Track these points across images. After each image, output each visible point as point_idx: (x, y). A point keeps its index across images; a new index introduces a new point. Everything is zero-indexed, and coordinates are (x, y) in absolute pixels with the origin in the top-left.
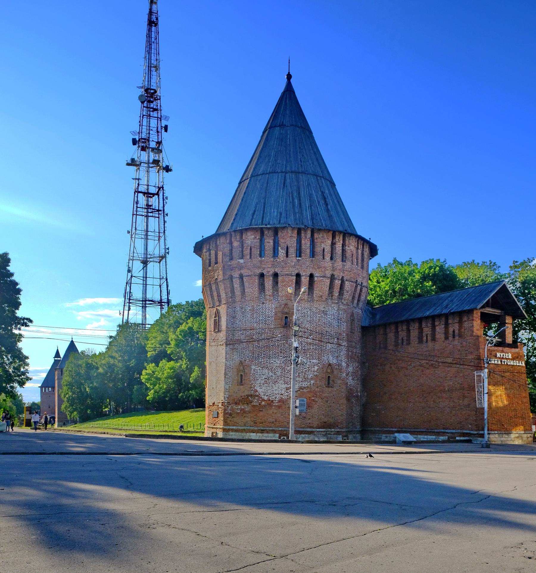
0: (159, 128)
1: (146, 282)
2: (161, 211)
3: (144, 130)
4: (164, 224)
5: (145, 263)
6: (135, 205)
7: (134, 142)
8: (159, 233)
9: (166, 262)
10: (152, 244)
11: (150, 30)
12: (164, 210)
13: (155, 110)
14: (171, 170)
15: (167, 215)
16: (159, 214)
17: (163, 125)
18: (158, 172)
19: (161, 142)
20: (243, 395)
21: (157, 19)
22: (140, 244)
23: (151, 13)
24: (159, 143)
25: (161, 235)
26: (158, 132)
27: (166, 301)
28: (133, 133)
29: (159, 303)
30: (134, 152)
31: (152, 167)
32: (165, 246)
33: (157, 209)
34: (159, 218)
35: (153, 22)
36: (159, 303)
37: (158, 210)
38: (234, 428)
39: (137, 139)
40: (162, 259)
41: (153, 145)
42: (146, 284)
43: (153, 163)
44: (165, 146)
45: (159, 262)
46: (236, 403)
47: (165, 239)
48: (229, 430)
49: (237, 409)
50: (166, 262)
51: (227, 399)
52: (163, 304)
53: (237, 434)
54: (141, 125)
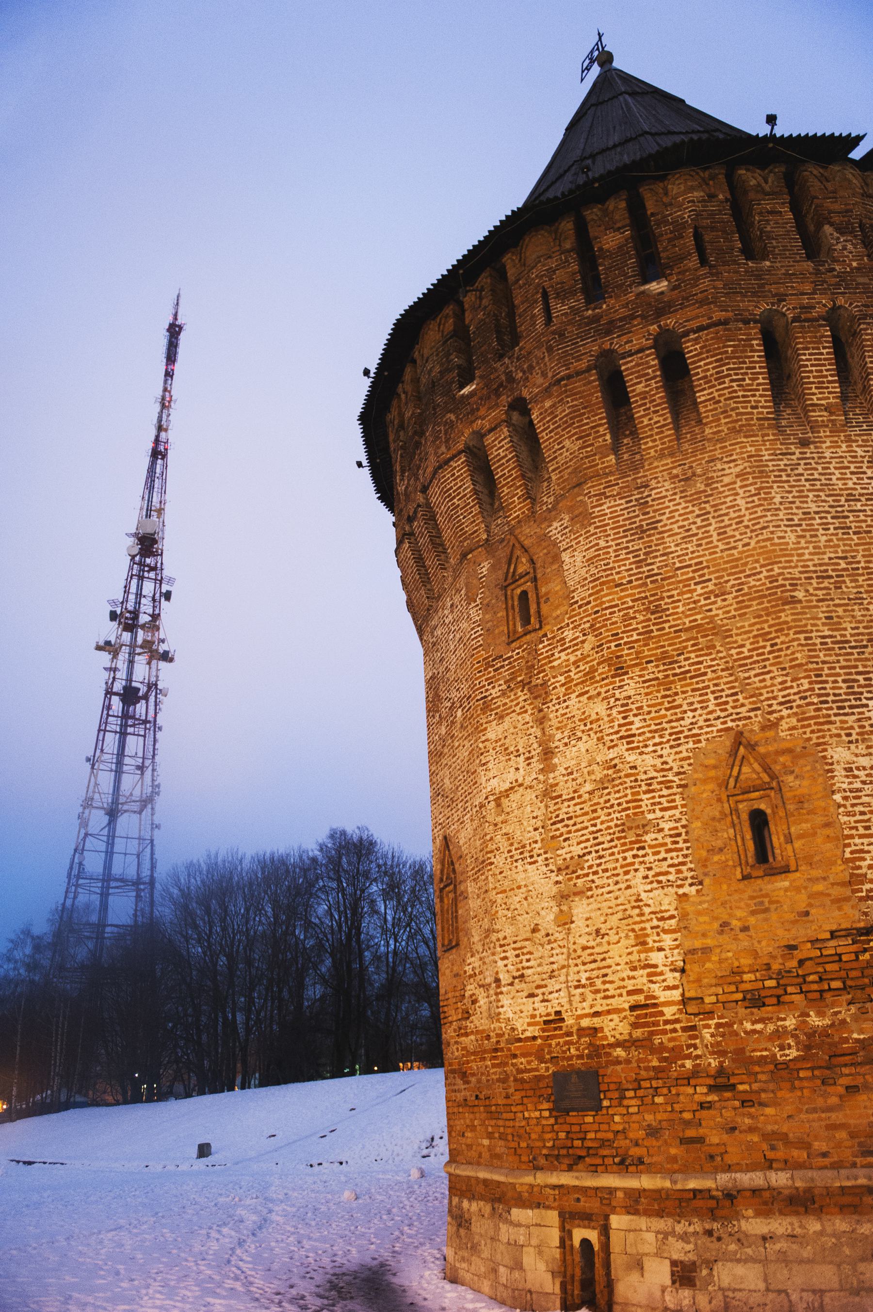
0: (158, 595)
1: (112, 847)
2: (149, 722)
3: (132, 597)
4: (154, 745)
5: (113, 813)
6: (105, 712)
7: (113, 616)
8: (143, 758)
9: (153, 809)
10: (128, 781)
11: (153, 464)
12: (155, 721)
13: (153, 569)
14: (171, 660)
15: (160, 729)
16: (146, 729)
17: (164, 591)
18: (149, 663)
19: (159, 615)
20: (801, 933)
21: (166, 449)
22: (106, 780)
23: (157, 440)
24: (155, 617)
25: (148, 762)
26: (154, 600)
27: (147, 880)
28: (113, 602)
29: (134, 884)
30: (111, 631)
31: (139, 654)
32: (153, 780)
33: (143, 718)
34: (144, 736)
35: (160, 453)
36: (134, 884)
37: (146, 722)
38: (780, 1179)
39: (119, 612)
40: (145, 806)
41: (144, 619)
42: (112, 853)
43: (141, 647)
44: (165, 621)
45: (140, 812)
46: (755, 1001)
47: (153, 770)
48: (731, 1196)
49: (779, 1034)
50: (153, 809)
51: (672, 978)
52: (142, 887)
53: (814, 1226)
54: (127, 591)
